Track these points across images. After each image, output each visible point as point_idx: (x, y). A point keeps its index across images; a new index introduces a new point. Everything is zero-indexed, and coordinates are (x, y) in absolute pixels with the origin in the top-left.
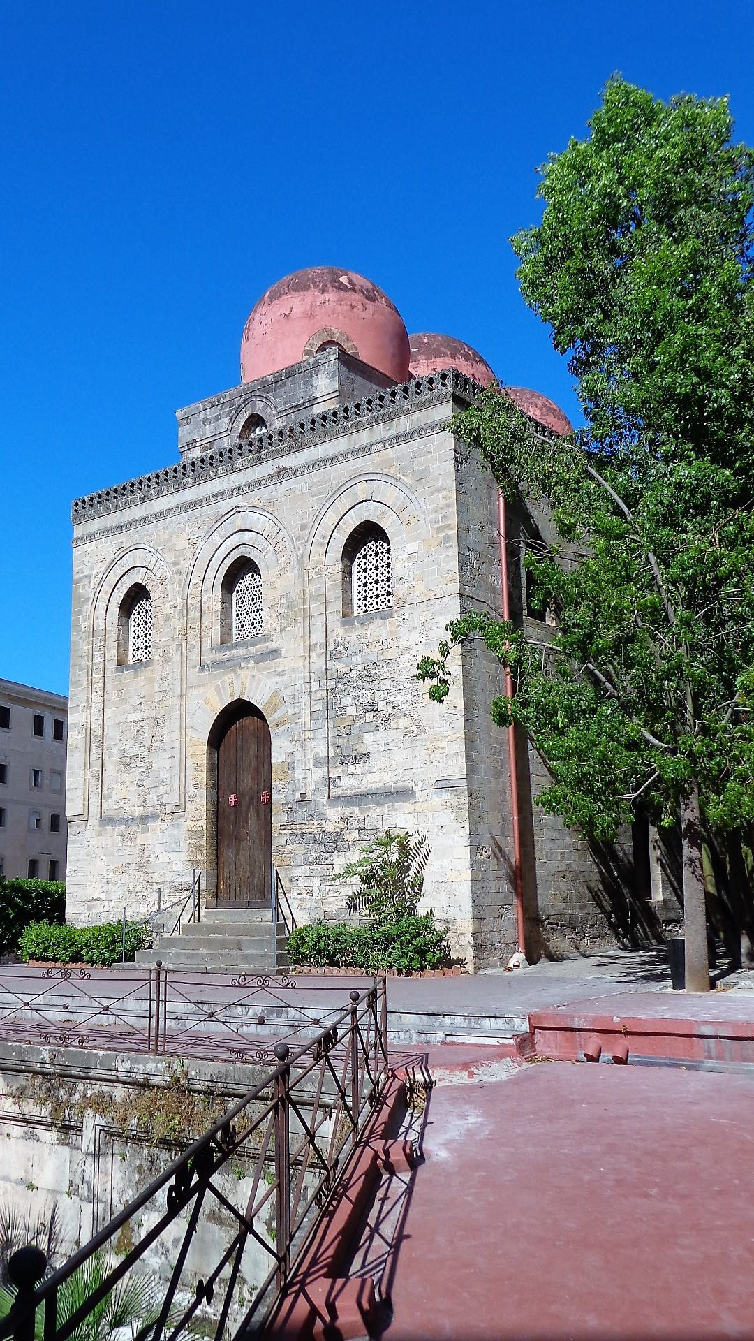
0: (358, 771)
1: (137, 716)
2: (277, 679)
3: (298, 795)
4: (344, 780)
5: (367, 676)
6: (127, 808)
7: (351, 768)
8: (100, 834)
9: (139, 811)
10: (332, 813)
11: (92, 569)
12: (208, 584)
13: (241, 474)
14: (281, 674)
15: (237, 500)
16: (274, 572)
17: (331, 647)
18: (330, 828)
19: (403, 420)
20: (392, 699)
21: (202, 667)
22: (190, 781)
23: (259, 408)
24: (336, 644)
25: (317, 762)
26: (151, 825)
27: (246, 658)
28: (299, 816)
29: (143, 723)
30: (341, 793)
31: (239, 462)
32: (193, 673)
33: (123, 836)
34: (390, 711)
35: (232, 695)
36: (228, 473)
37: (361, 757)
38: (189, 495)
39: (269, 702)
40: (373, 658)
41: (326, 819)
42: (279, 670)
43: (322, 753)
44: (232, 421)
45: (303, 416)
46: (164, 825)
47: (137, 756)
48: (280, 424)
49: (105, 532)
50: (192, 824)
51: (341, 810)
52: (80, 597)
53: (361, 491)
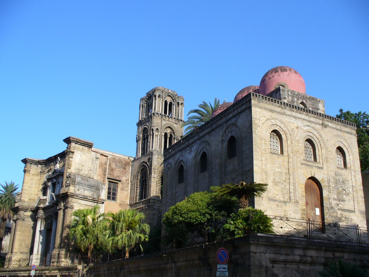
0: (343, 203)
1: (280, 171)
2: (323, 175)
3: (331, 206)
4: (340, 205)
5: (343, 182)
6: (277, 197)
7: (341, 203)
8: (268, 203)
9: (282, 199)
10: (339, 212)
11: (260, 117)
12: (301, 141)
13: (310, 118)
14: (324, 174)
15: (309, 124)
16: (319, 147)
17: (335, 172)
18: (339, 216)
19: (347, 129)
20: (349, 189)
21: (302, 164)
22: (300, 194)
23: (304, 101)
24: (336, 172)
25: (334, 199)
26: (287, 204)
27: (315, 167)
28: (331, 211)
29: (282, 173)
30: (339, 208)
31: (310, 114)
32: (299, 164)
33: (277, 205)
34: (348, 192)
35: (311, 174)
36: (306, 115)
37: (343, 201)
38: (294, 114)
39: (322, 180)
40: (344, 179)
41: (337, 213)
42: (324, 173)
43: (336, 197)
44: (297, 100)
45: (316, 111)
46: (292, 205)
47: (280, 182)
48: (310, 109)
49: (266, 109)
50: (302, 207)
51: (341, 212)
52: (256, 124)
53: (339, 139)
